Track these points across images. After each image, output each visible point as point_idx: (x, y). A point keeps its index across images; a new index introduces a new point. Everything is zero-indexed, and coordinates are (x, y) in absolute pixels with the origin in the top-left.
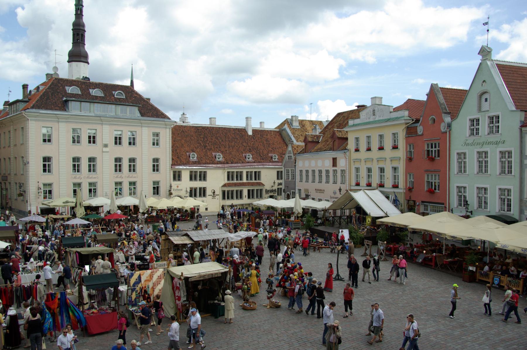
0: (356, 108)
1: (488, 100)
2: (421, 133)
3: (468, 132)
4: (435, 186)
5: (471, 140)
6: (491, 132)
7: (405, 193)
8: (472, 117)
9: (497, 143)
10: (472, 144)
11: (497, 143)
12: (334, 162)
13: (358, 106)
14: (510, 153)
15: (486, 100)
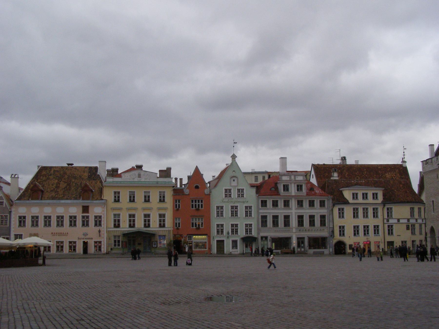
0: (67, 166)
1: (236, 181)
2: (187, 194)
3: (224, 196)
4: (199, 225)
5: (226, 200)
6: (239, 196)
7: (173, 231)
8: (226, 188)
9: (243, 202)
10: (228, 202)
11: (243, 202)
12: (86, 209)
13: (68, 164)
14: (251, 207)
15: (234, 180)
